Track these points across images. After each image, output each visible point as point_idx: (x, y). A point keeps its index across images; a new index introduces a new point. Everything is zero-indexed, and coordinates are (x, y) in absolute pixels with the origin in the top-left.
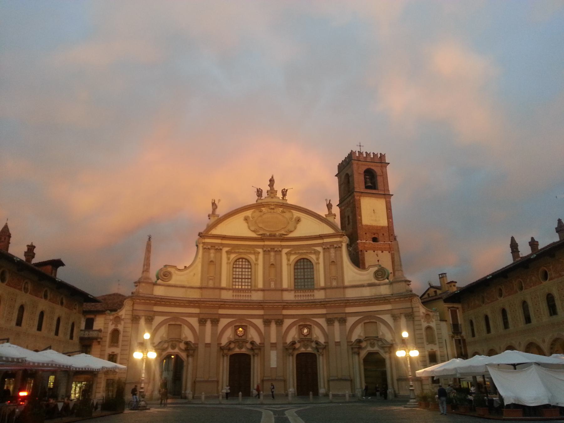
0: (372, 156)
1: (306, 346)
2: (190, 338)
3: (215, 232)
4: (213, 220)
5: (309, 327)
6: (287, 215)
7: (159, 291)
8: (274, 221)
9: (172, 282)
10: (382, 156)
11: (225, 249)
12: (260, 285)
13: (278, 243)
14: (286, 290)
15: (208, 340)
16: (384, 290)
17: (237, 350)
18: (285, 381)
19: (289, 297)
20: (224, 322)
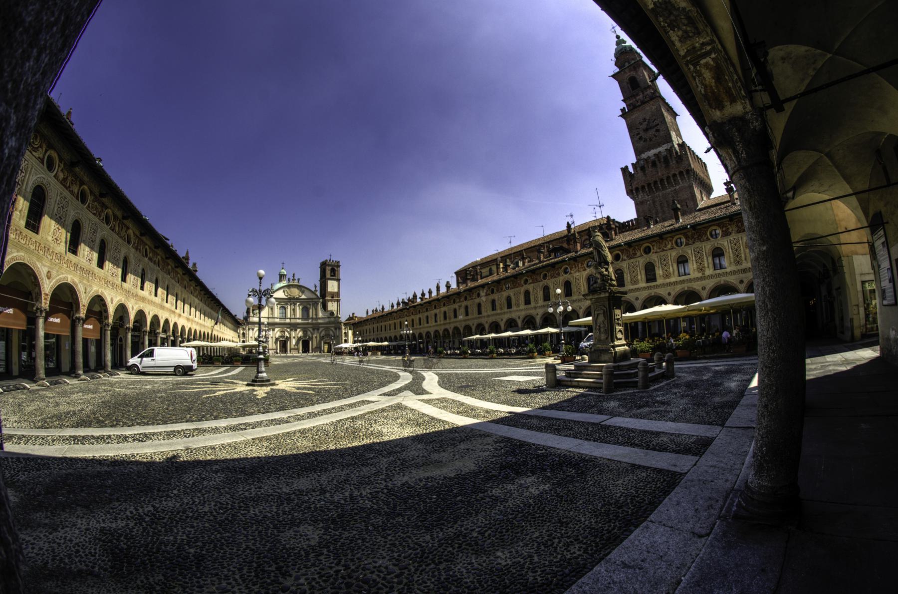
16: (332, 319)
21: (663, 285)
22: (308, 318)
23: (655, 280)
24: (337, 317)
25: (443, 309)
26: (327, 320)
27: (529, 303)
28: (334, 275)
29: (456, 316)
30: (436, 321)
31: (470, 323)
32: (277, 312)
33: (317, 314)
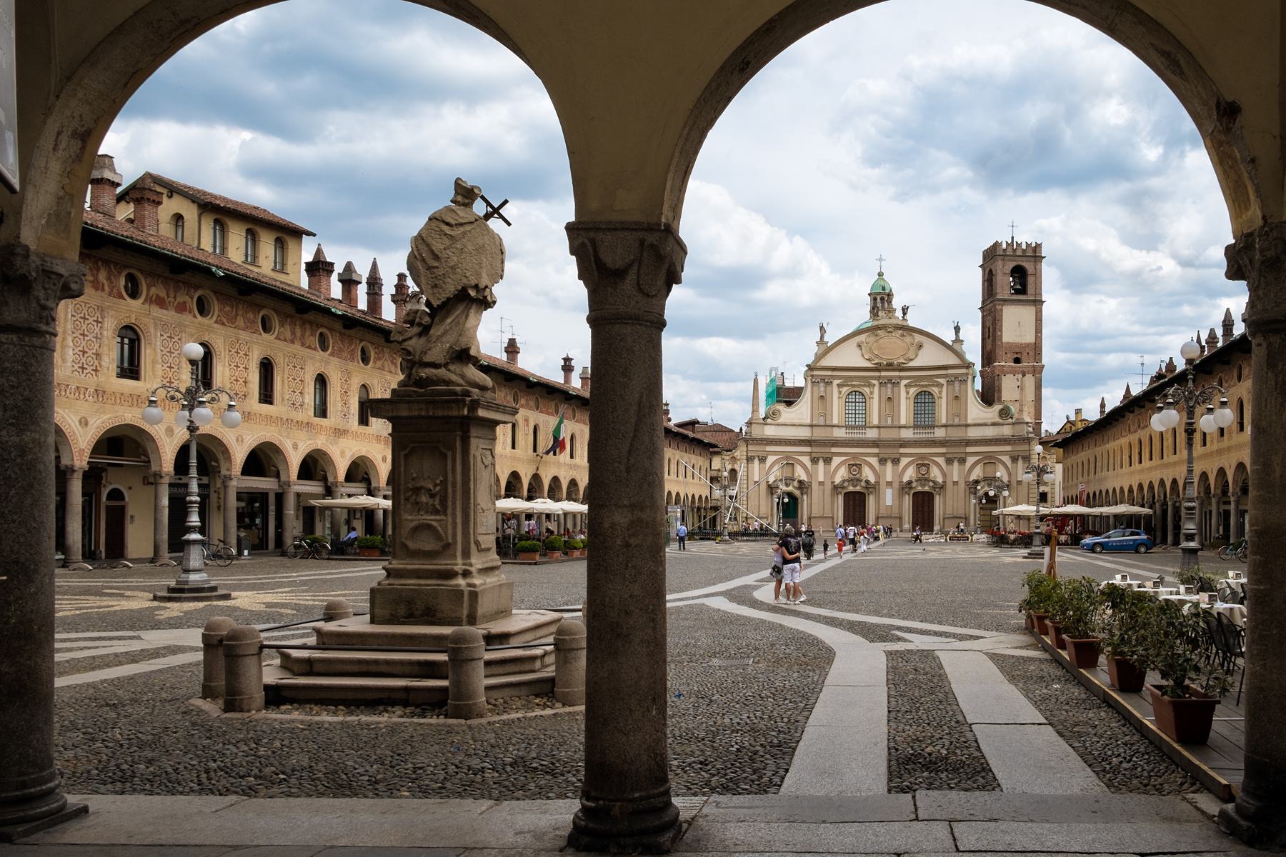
0: (1024, 246)
1: (923, 486)
2: (804, 477)
3: (824, 363)
4: (824, 347)
5: (927, 466)
6: (908, 339)
7: (770, 431)
8: (893, 348)
9: (781, 421)
10: (1038, 246)
11: (836, 382)
12: (876, 422)
13: (897, 374)
14: (905, 427)
15: (821, 479)
17: (851, 489)
18: (900, 518)
19: (907, 434)
20: (836, 461)
28: (1022, 290)
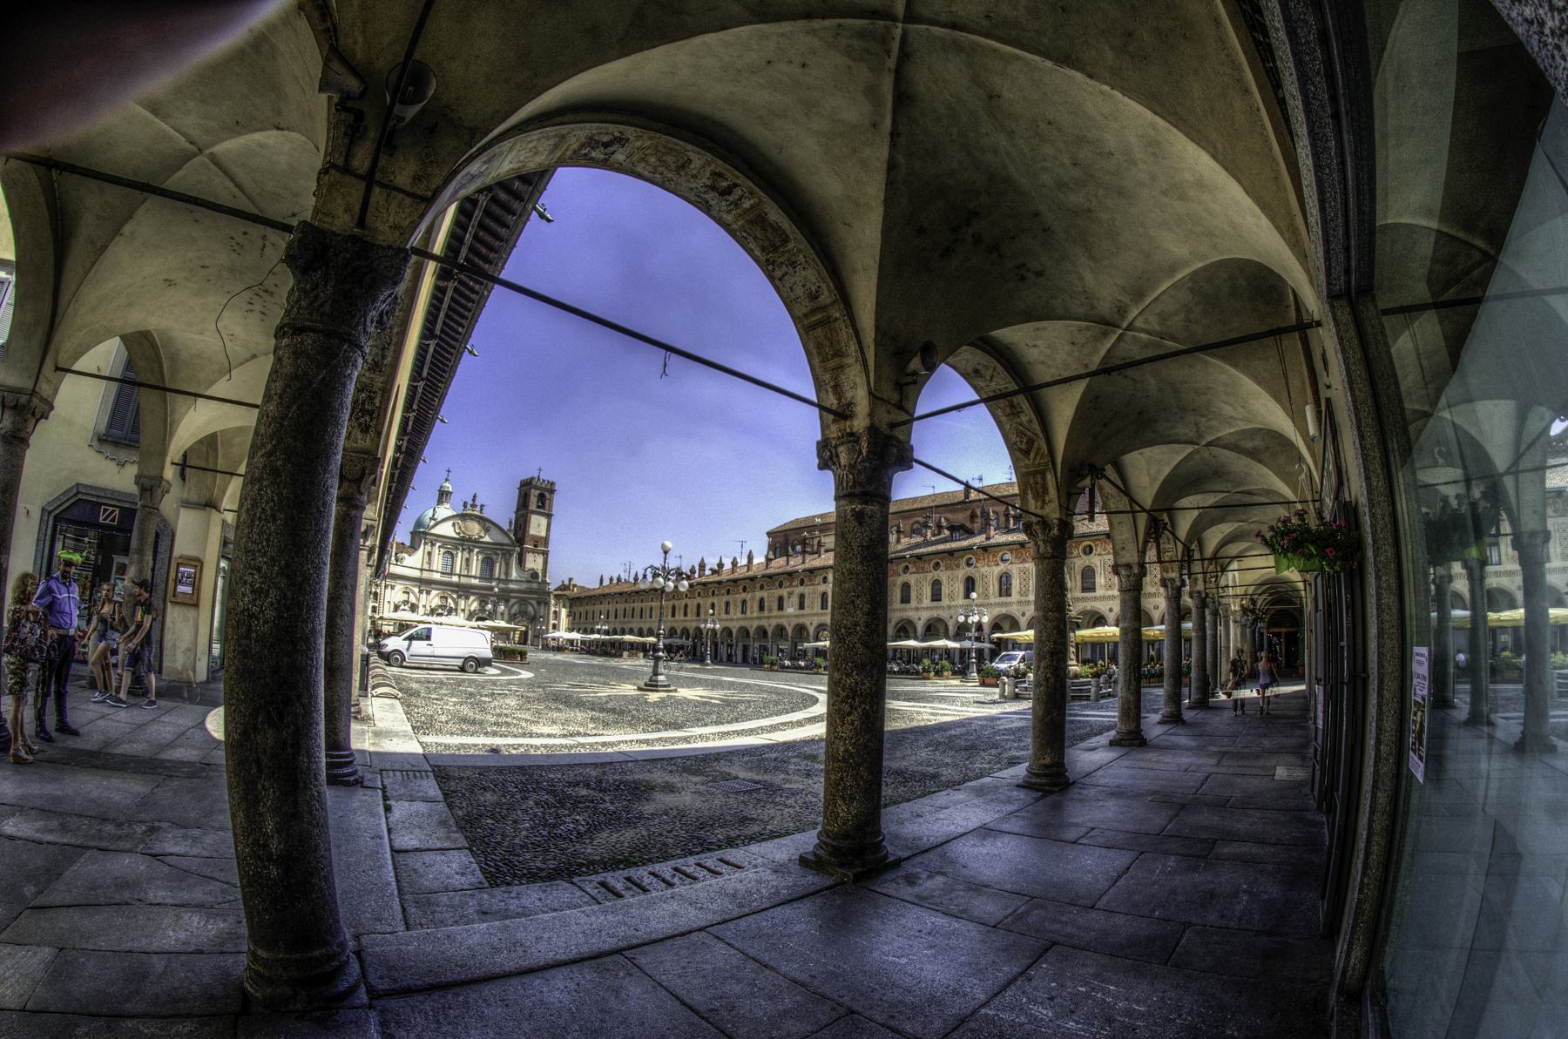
10: (553, 484)
16: (535, 586)
21: (1104, 598)
22: (491, 579)
23: (1093, 589)
24: (544, 582)
25: (759, 594)
26: (524, 586)
27: (908, 601)
28: (543, 506)
29: (781, 607)
30: (744, 612)
31: (806, 621)
32: (438, 561)
33: (507, 573)
